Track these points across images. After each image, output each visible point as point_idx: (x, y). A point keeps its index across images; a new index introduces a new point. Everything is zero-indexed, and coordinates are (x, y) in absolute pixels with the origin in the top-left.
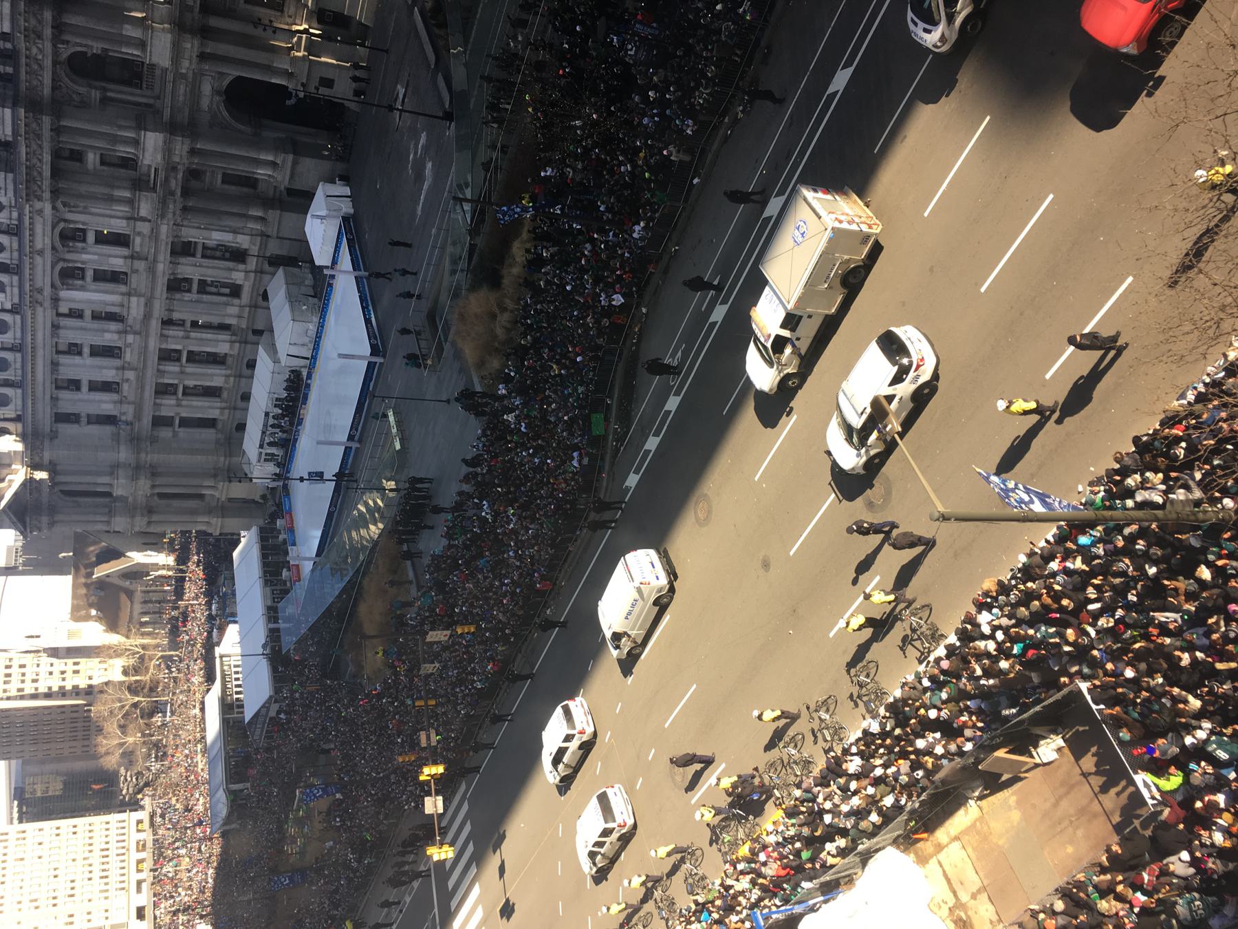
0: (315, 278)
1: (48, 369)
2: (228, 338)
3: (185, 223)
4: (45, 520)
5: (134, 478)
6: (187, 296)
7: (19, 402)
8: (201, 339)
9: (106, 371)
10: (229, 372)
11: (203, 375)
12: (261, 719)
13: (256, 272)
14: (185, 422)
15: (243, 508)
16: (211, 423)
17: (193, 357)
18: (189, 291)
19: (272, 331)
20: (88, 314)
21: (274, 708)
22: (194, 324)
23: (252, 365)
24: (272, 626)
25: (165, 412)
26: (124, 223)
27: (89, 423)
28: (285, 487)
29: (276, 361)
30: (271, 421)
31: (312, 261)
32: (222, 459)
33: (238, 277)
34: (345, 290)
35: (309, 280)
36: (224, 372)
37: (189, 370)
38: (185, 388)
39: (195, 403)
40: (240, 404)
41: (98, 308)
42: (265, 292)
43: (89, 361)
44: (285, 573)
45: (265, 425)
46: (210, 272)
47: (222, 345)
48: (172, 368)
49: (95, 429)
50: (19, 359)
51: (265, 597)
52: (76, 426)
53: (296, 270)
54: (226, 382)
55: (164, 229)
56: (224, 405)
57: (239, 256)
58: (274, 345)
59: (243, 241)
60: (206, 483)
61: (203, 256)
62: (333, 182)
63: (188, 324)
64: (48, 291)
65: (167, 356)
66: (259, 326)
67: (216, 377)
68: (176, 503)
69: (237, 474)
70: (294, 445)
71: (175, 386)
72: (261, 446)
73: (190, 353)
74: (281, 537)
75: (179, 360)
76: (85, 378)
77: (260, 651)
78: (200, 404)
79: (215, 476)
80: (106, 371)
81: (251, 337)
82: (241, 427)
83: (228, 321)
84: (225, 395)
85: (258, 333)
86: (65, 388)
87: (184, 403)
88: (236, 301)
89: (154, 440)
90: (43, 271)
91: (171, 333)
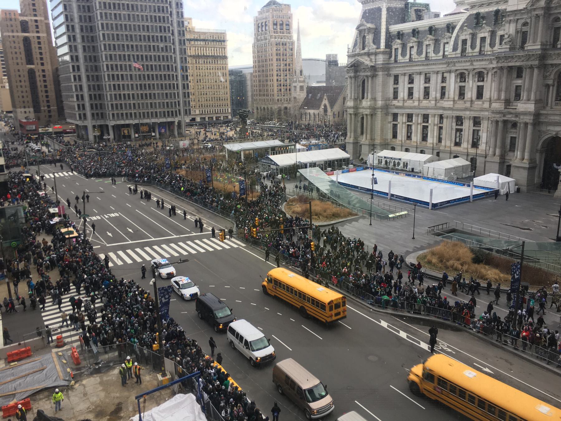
0: (465, 178)
1: (418, 71)
2: (435, 142)
3: (490, 122)
4: (352, 75)
5: (370, 108)
6: (454, 124)
7: (403, 61)
8: (434, 131)
9: (418, 92)
10: (419, 143)
11: (417, 131)
12: (270, 162)
13: (468, 152)
14: (395, 126)
15: (357, 152)
16: (395, 136)
17: (425, 128)
18: (457, 125)
19: (439, 160)
20: (444, 85)
21: (274, 167)
22: (441, 128)
23: (422, 152)
24: (308, 165)
25: (400, 118)
26: (488, 97)
27: (394, 88)
28: (367, 168)
29: (425, 162)
30: (397, 161)
31: (474, 176)
32: (379, 142)
33: (464, 145)
34: (463, 192)
35: (464, 175)
36: (419, 140)
37: (419, 126)
38: (411, 125)
39: (404, 130)
40: (404, 148)
41: (447, 88)
42: (458, 157)
43: (422, 87)
44: (330, 169)
45: (395, 159)
46: (467, 133)
47: (432, 139)
48: (420, 120)
49: (391, 91)
50: (422, 59)
51: (321, 161)
52: (393, 83)
53: (470, 170)
54: (414, 142)
55: (487, 113)
56: (403, 141)
57: (475, 145)
58: (433, 161)
59: (482, 146)
60: (368, 136)
61: (474, 130)
62: (516, 185)
63: (441, 125)
64: (454, 68)
65: (426, 118)
66: (441, 154)
67: (416, 137)
68: (359, 125)
69: (373, 148)
70: (386, 171)
71: (411, 121)
72: (385, 157)
73: (427, 127)
74: (345, 167)
75: (424, 122)
76: (415, 86)
77: (298, 161)
78: (404, 132)
79: (371, 139)
80: (418, 92)
81: (435, 152)
82: (393, 149)
83: (443, 142)
84: (408, 142)
85: (438, 154)
86: (410, 79)
87: (404, 125)
88: (453, 145)
89: (387, 114)
90: (461, 66)
91: (436, 118)
